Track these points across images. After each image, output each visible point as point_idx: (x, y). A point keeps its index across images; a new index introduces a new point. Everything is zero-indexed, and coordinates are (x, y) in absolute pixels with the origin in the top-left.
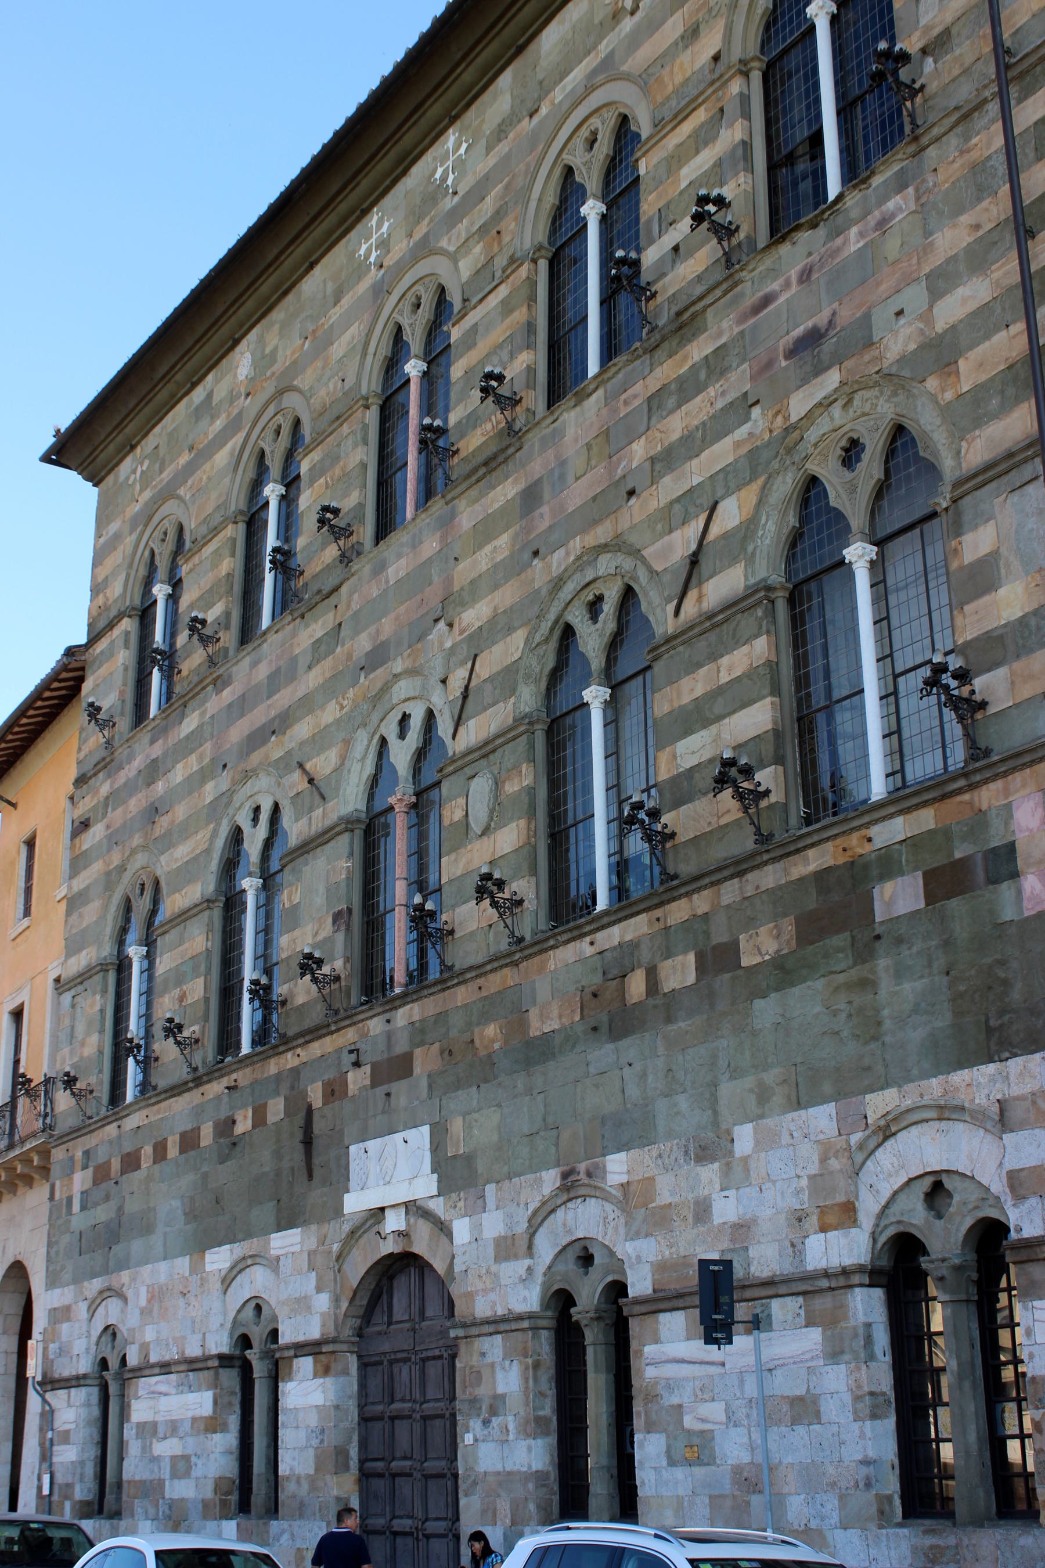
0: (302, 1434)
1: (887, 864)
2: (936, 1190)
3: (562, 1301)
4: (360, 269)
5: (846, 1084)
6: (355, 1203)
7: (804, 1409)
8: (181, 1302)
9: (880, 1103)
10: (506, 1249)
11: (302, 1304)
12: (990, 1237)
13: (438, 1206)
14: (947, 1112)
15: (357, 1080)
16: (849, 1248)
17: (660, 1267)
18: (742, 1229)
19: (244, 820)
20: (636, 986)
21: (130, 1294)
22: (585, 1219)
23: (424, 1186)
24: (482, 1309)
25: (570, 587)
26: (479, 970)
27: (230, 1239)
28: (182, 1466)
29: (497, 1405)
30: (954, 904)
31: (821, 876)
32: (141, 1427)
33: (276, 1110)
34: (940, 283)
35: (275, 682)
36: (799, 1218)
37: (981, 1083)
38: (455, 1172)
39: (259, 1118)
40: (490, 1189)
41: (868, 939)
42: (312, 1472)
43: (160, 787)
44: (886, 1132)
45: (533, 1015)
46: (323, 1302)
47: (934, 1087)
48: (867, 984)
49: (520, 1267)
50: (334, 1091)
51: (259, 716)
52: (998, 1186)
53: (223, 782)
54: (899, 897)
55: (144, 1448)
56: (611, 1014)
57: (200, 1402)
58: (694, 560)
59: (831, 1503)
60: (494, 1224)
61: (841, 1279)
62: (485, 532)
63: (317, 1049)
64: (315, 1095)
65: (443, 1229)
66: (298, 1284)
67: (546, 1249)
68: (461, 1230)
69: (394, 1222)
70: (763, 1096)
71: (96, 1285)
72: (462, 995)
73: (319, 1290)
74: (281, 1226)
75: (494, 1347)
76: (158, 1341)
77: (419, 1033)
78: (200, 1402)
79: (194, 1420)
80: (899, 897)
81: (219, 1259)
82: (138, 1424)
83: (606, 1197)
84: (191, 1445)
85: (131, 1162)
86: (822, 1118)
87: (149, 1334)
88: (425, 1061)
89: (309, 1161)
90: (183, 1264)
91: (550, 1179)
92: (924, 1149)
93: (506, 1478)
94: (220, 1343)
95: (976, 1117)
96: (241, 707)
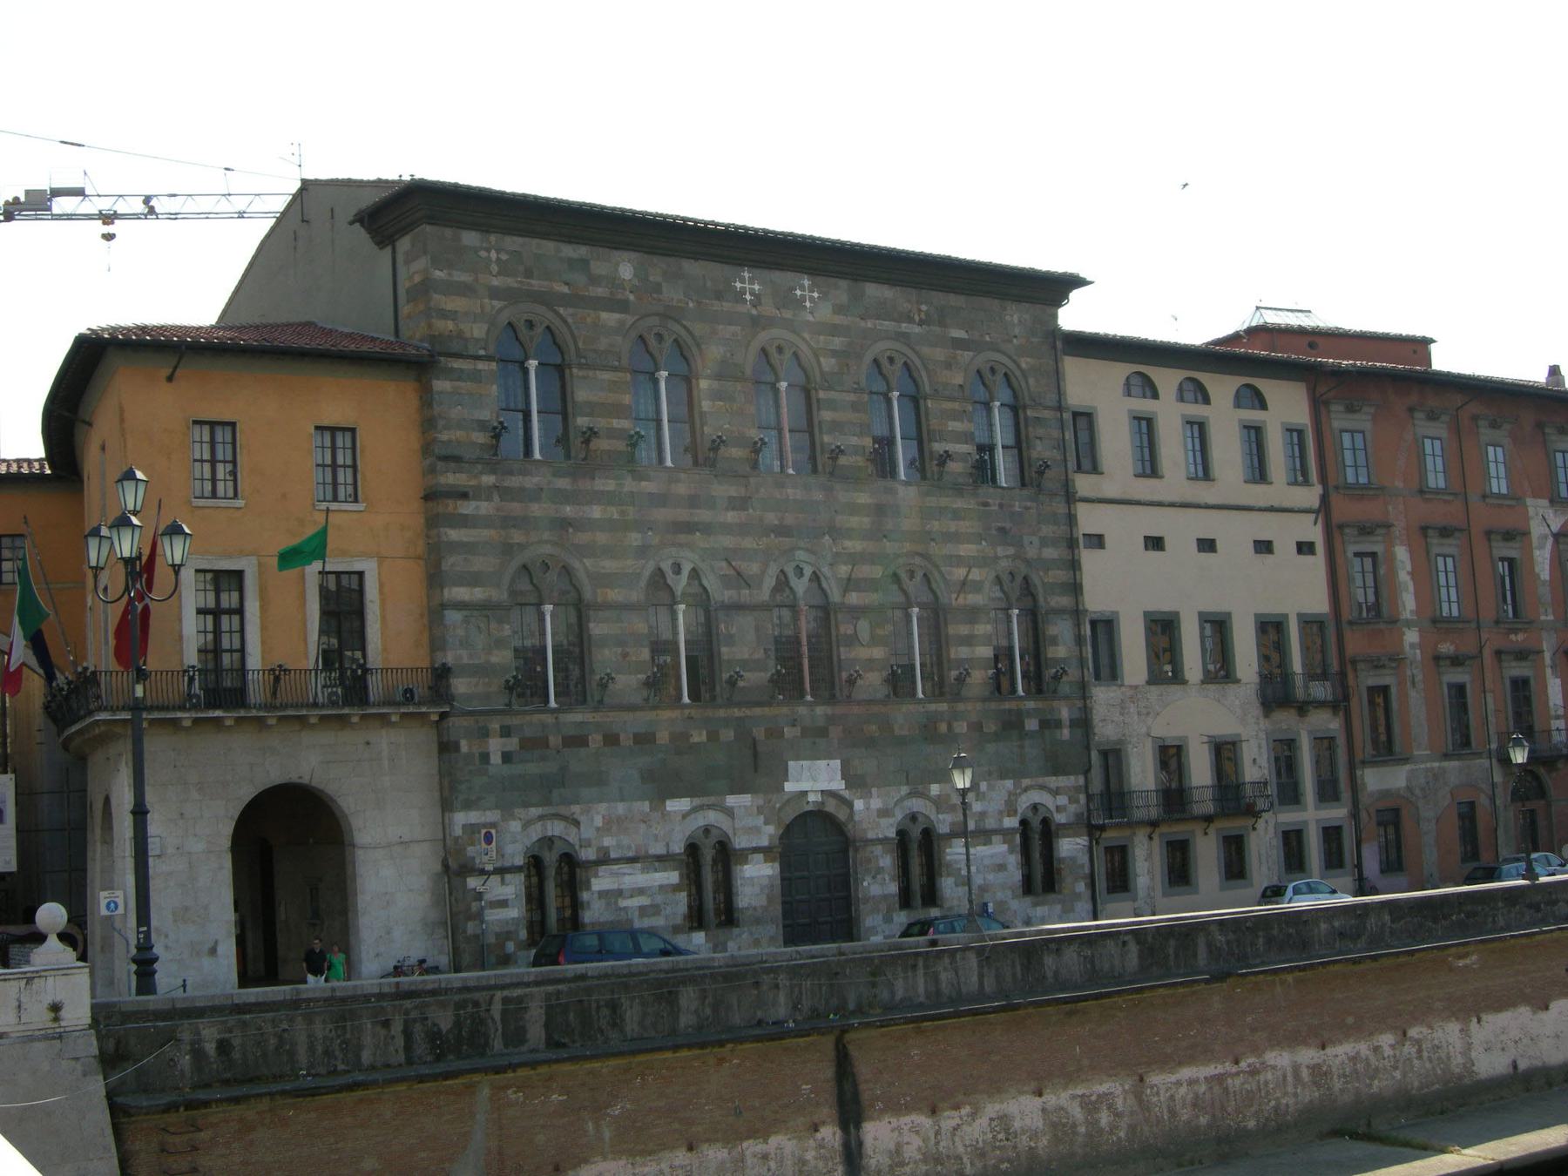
0: (757, 889)
1: (1029, 714)
2: (1035, 807)
3: (902, 833)
4: (739, 297)
5: (1017, 775)
6: (789, 787)
7: (1001, 867)
8: (643, 826)
9: (1026, 782)
10: (884, 813)
11: (756, 830)
12: (1046, 822)
13: (846, 794)
14: (1042, 787)
15: (788, 732)
16: (1011, 822)
17: (952, 824)
18: (983, 814)
19: (666, 566)
20: (943, 728)
21: (582, 819)
22: (917, 805)
23: (838, 785)
24: (871, 835)
25: (901, 561)
26: (870, 702)
27: (690, 793)
28: (654, 910)
29: (880, 870)
30: (1047, 732)
31: (1010, 711)
32: (603, 894)
33: (728, 735)
34: (1044, 542)
35: (693, 502)
36: (1001, 813)
37: (1053, 782)
38: (854, 780)
39: (713, 736)
40: (874, 790)
41: (1024, 735)
42: (764, 902)
43: (568, 510)
44: (1026, 790)
45: (896, 727)
46: (770, 829)
47: (1040, 780)
48: (1022, 747)
49: (891, 820)
50: (775, 733)
51: (682, 514)
52: (1053, 808)
53: (654, 538)
54: (1032, 725)
55: (608, 904)
56: (929, 732)
57: (673, 877)
58: (964, 583)
59: (1009, 893)
60: (876, 803)
61: (1011, 831)
62: (854, 509)
63: (758, 711)
64: (759, 733)
65: (850, 805)
66: (748, 820)
67: (899, 815)
68: (859, 805)
69: (812, 798)
70: (990, 773)
71: (534, 811)
72: (856, 710)
73: (766, 823)
74: (732, 793)
75: (878, 850)
76: (619, 846)
77: (831, 720)
78: (673, 877)
79: (661, 887)
80: (1032, 725)
81: (678, 805)
82: (600, 893)
83: (928, 798)
84: (659, 899)
85: (577, 741)
86: (1009, 784)
87: (607, 841)
88: (835, 732)
89: (756, 766)
90: (646, 806)
91: (905, 790)
92: (1036, 797)
93: (885, 897)
94: (678, 848)
95: (1050, 790)
96: (661, 500)
